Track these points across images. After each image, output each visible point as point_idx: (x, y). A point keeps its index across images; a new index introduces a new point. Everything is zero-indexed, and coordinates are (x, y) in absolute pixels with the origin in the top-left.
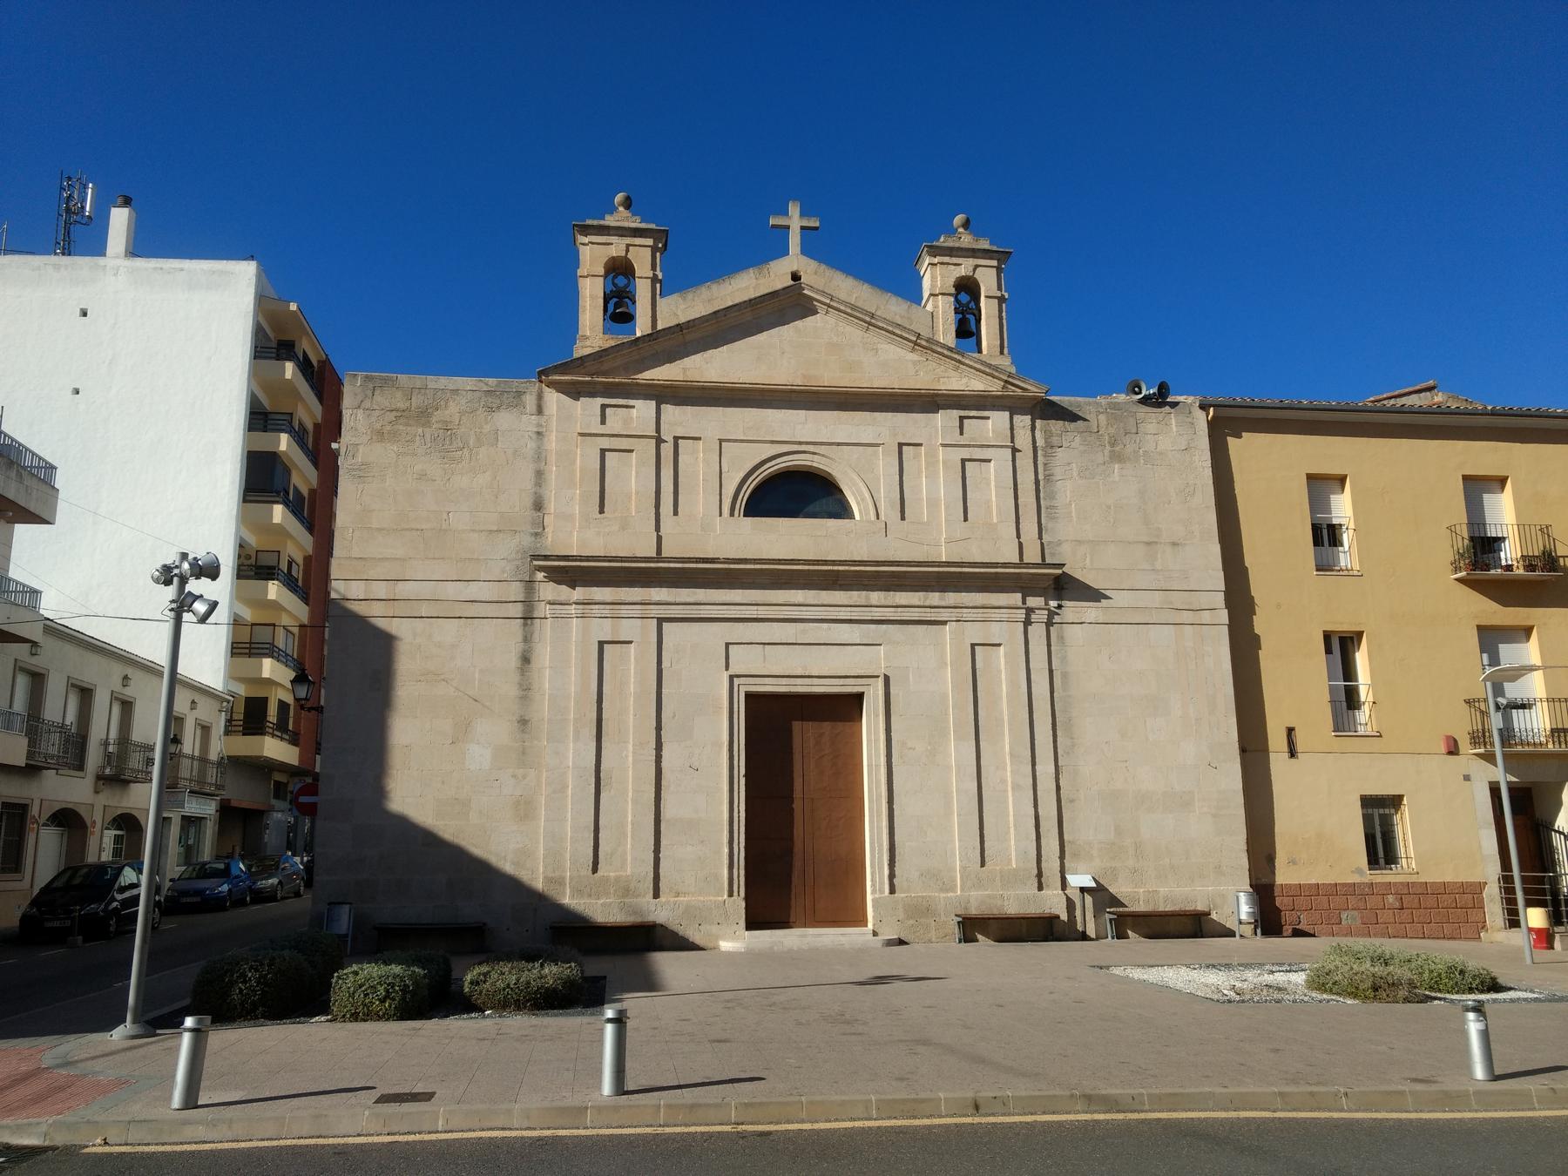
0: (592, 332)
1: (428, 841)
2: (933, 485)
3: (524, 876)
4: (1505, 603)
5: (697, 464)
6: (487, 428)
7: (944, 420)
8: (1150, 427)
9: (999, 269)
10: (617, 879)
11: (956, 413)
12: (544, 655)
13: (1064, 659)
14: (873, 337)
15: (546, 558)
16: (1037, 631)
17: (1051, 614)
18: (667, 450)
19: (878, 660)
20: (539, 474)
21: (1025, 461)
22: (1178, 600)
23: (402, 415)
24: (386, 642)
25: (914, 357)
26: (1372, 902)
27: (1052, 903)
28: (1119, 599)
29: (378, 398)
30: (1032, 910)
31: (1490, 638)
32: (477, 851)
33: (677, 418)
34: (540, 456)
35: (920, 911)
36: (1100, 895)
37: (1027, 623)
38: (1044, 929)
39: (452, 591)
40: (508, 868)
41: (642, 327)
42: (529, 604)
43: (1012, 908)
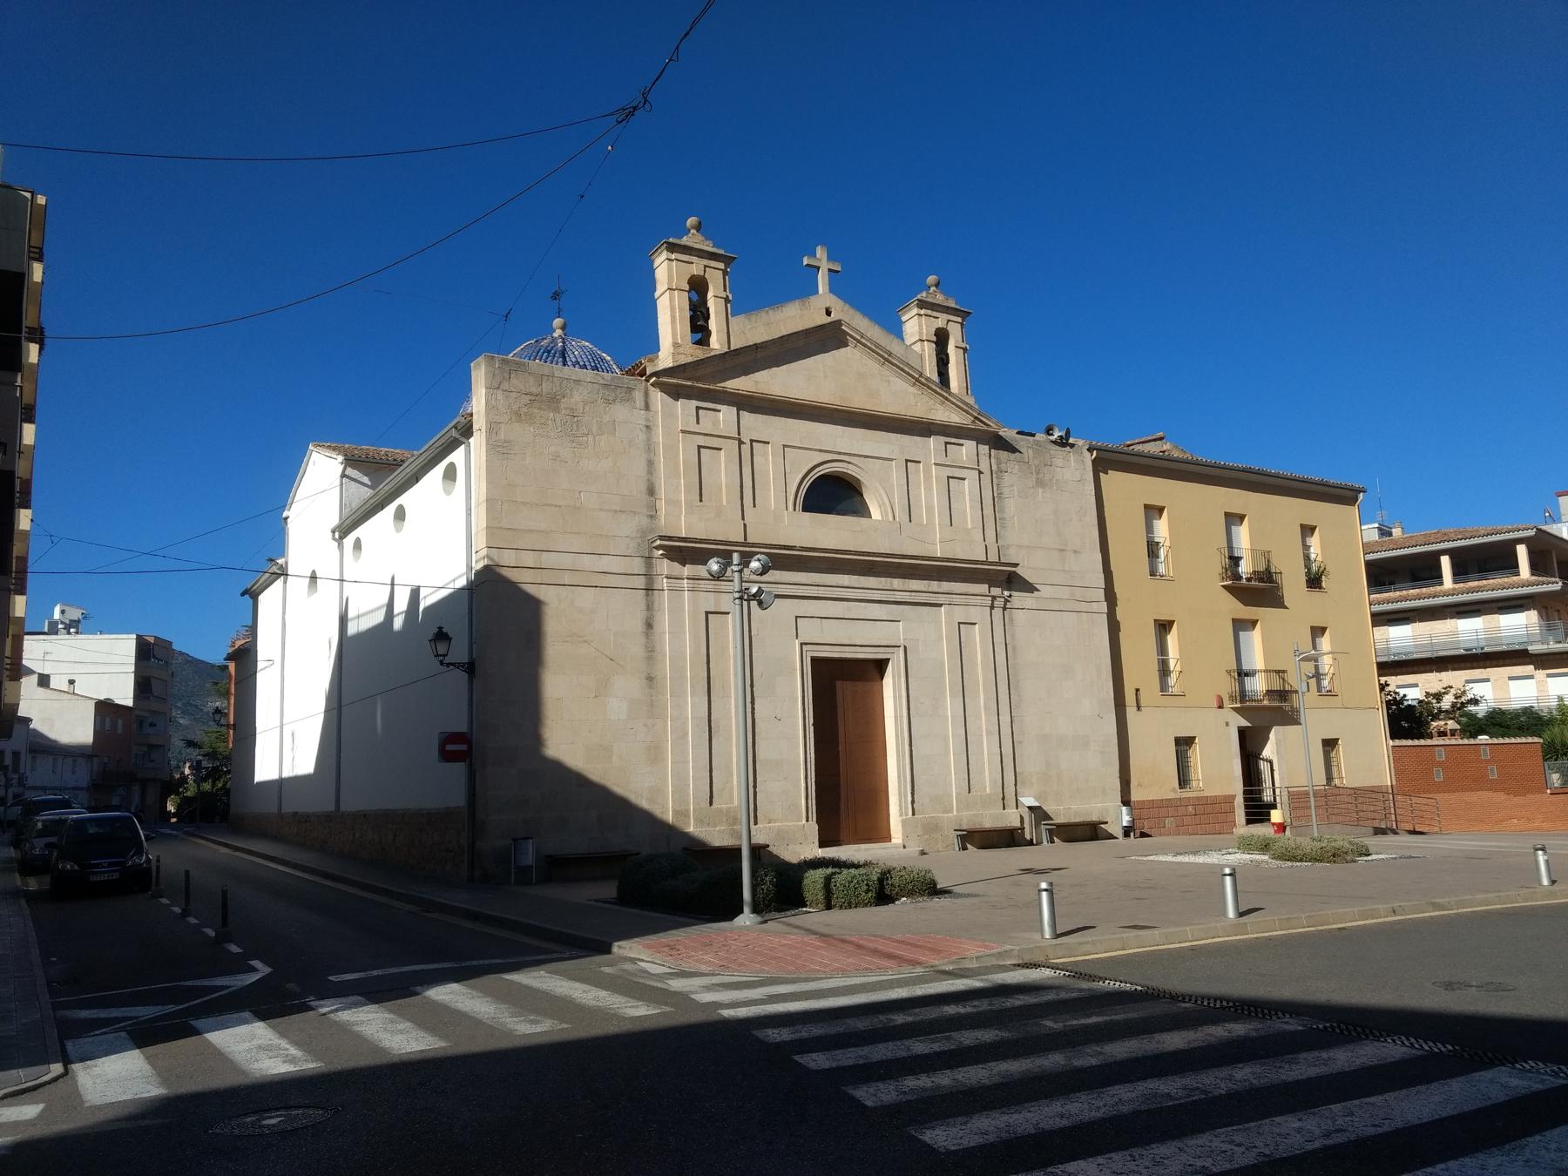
0: (671, 340)
1: (579, 781)
2: (929, 495)
3: (657, 811)
4: (1246, 604)
5: (768, 461)
6: (606, 418)
7: (934, 443)
8: (1058, 461)
9: (725, 273)
10: (728, 810)
11: (943, 439)
12: (664, 622)
13: (1013, 636)
14: (887, 371)
15: (670, 538)
16: (998, 612)
17: (1006, 601)
18: (746, 449)
19: (899, 632)
20: (651, 464)
21: (986, 478)
22: (1078, 593)
23: (535, 398)
24: (533, 608)
25: (913, 390)
26: (1181, 811)
27: (1011, 818)
28: (1045, 591)
29: (514, 381)
30: (1000, 824)
31: (1240, 625)
32: (618, 789)
33: (755, 424)
34: (650, 448)
35: (931, 828)
36: (1038, 813)
37: (992, 607)
38: (1009, 838)
39: (588, 562)
40: (644, 804)
41: (716, 344)
42: (649, 576)
43: (988, 824)
